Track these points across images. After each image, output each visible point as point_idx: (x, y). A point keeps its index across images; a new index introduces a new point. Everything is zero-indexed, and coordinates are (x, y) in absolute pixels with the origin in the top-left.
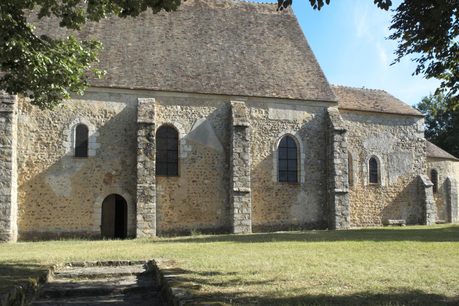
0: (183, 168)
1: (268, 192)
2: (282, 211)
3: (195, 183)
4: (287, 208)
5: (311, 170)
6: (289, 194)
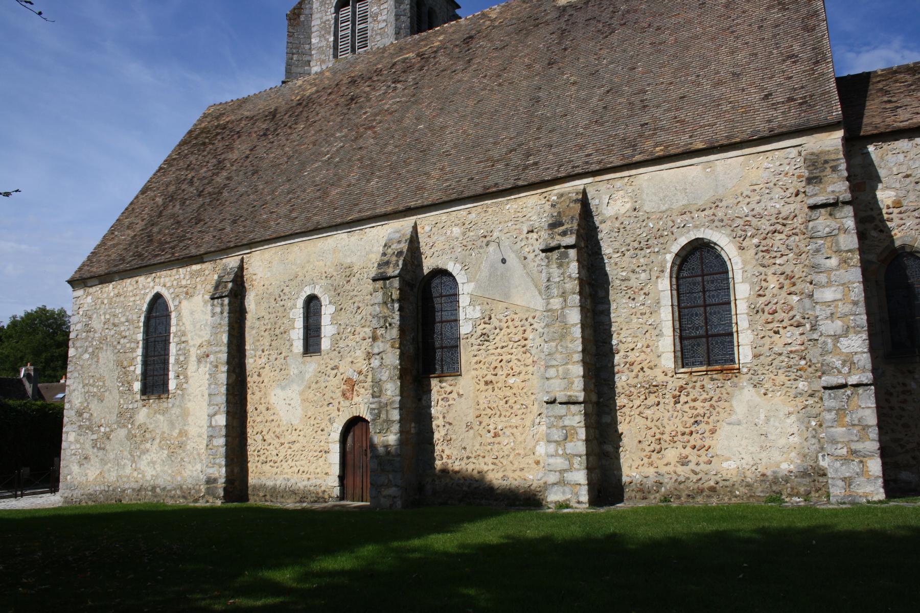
0: (466, 355)
1: (652, 396)
2: (692, 443)
3: (490, 386)
4: (707, 434)
5: (770, 326)
6: (711, 399)
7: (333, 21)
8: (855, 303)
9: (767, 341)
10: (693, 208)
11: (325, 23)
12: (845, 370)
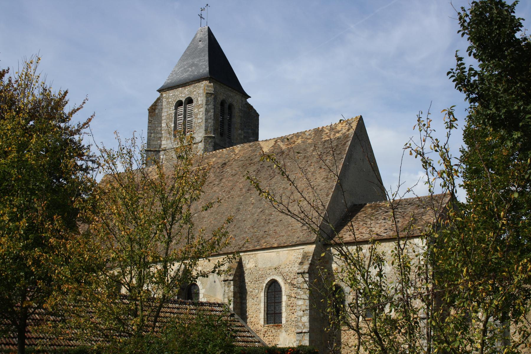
7: (174, 115)
8: (307, 306)
9: (290, 316)
10: (272, 268)
11: (169, 115)
12: (303, 327)
